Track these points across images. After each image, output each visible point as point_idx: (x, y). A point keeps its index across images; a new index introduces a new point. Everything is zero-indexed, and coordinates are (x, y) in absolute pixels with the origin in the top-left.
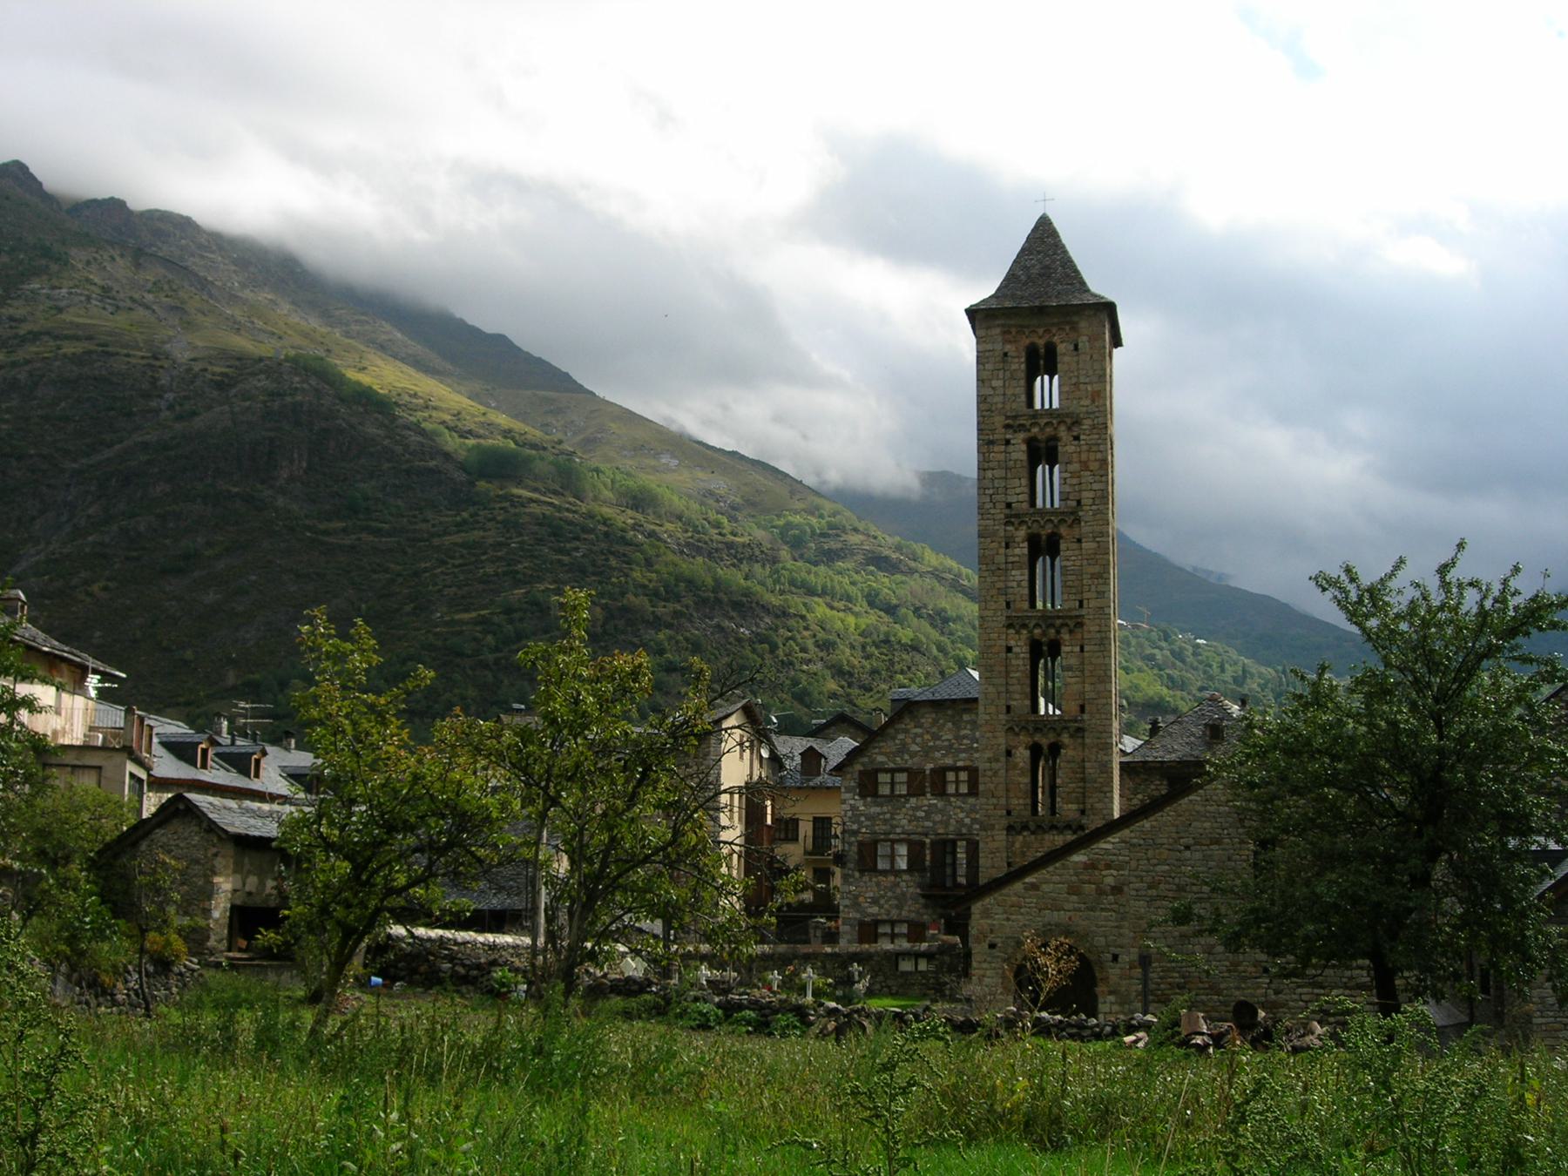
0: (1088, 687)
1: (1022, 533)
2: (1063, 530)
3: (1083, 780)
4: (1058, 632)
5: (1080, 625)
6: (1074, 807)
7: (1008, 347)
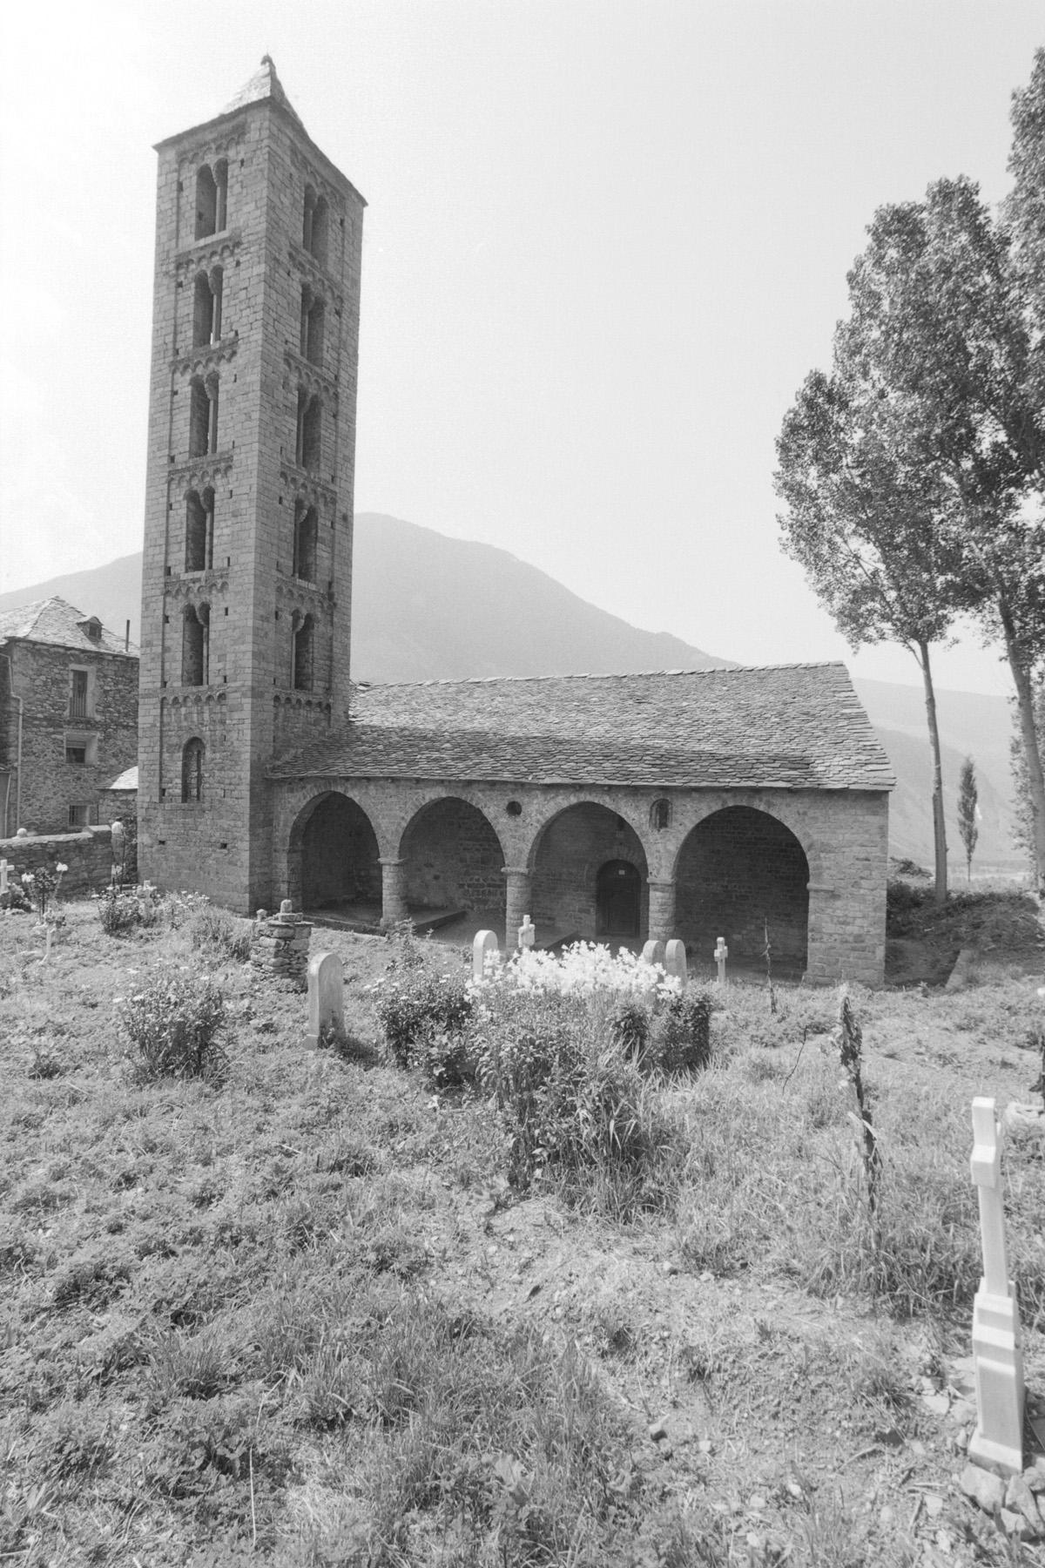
0: (337, 567)
1: (294, 380)
2: (323, 396)
3: (330, 658)
4: (317, 500)
5: (334, 502)
6: (321, 684)
7: (293, 170)
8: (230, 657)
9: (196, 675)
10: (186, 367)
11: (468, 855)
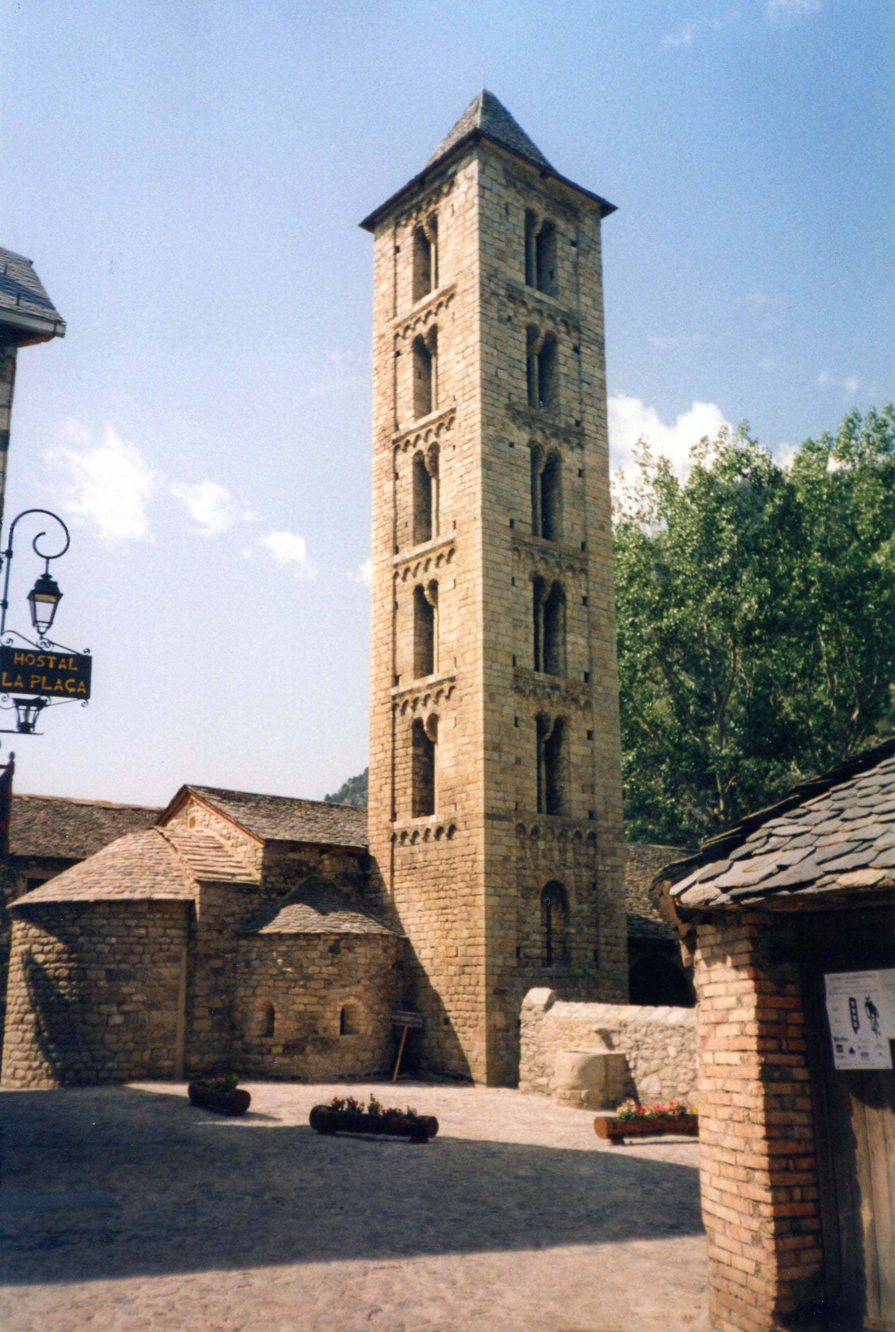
8: (599, 790)
9: (551, 799)
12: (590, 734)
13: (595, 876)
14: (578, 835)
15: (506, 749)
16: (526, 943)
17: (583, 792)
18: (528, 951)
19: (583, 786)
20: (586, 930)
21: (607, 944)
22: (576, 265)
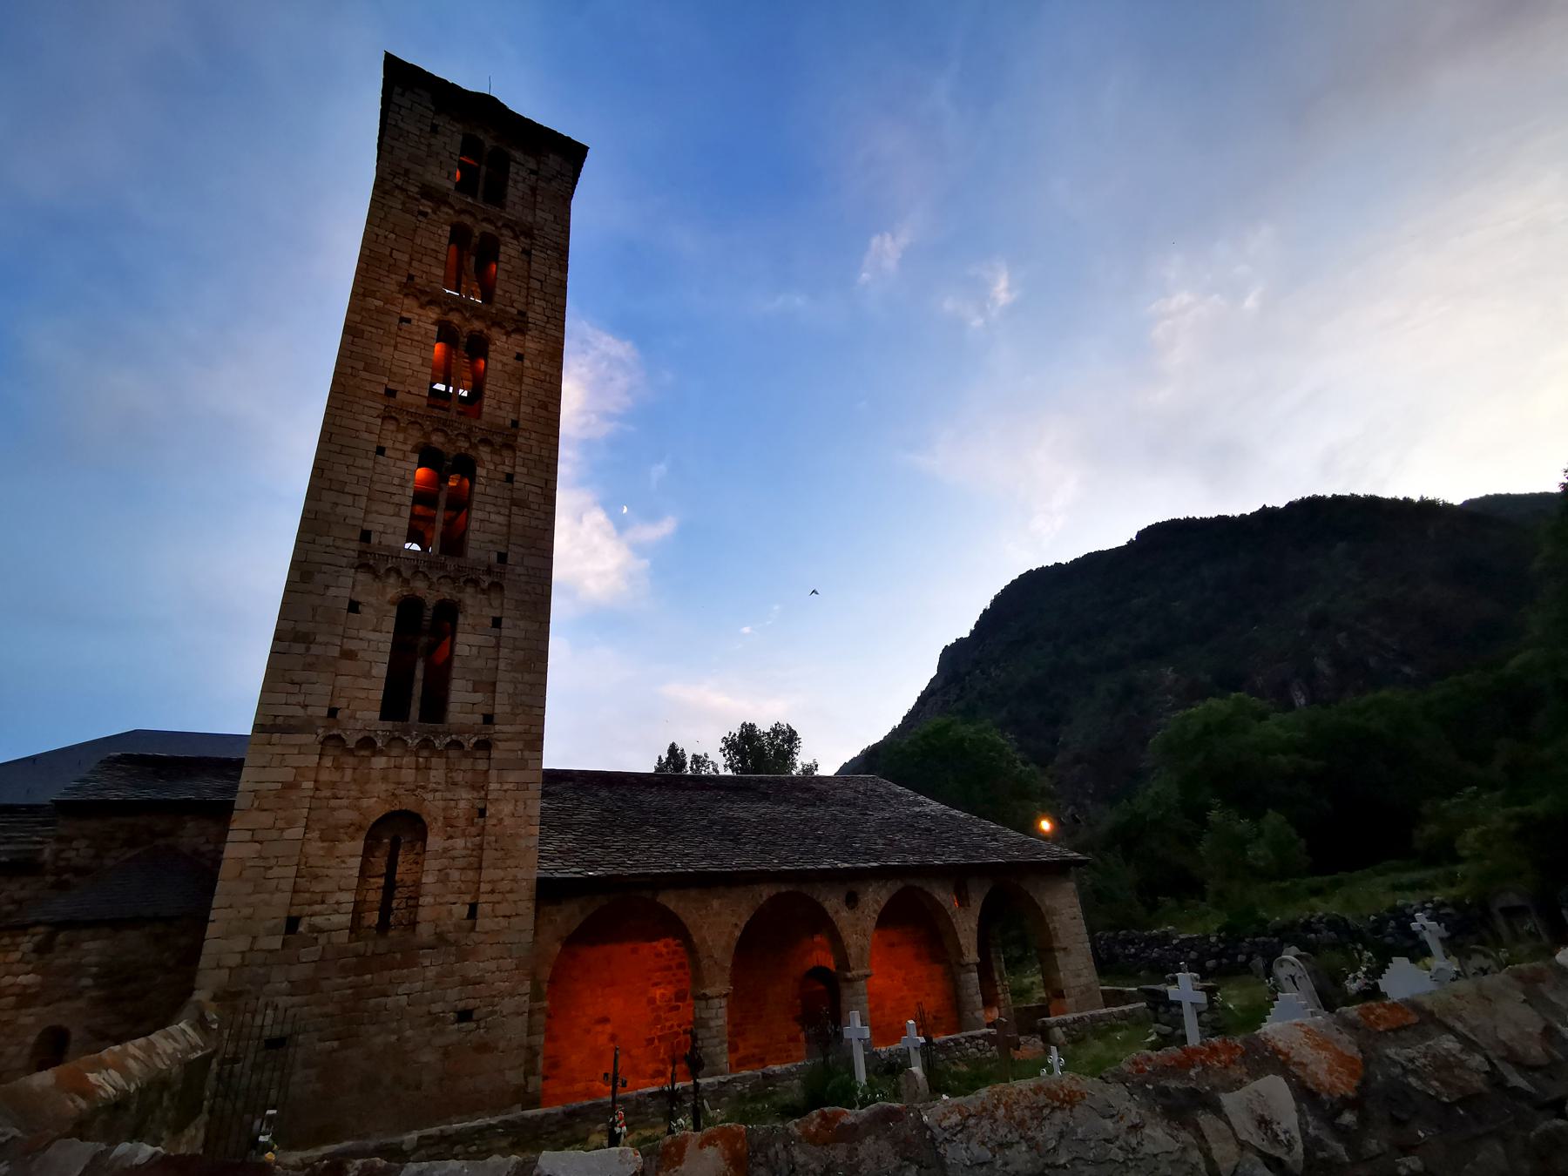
10: (430, 303)
11: (658, 992)
12: (497, 622)
13: (485, 798)
14: (457, 745)
15: (319, 638)
16: (317, 908)
17: (475, 691)
18: (318, 920)
19: (475, 683)
20: (455, 875)
21: (492, 892)
22: (534, 190)
